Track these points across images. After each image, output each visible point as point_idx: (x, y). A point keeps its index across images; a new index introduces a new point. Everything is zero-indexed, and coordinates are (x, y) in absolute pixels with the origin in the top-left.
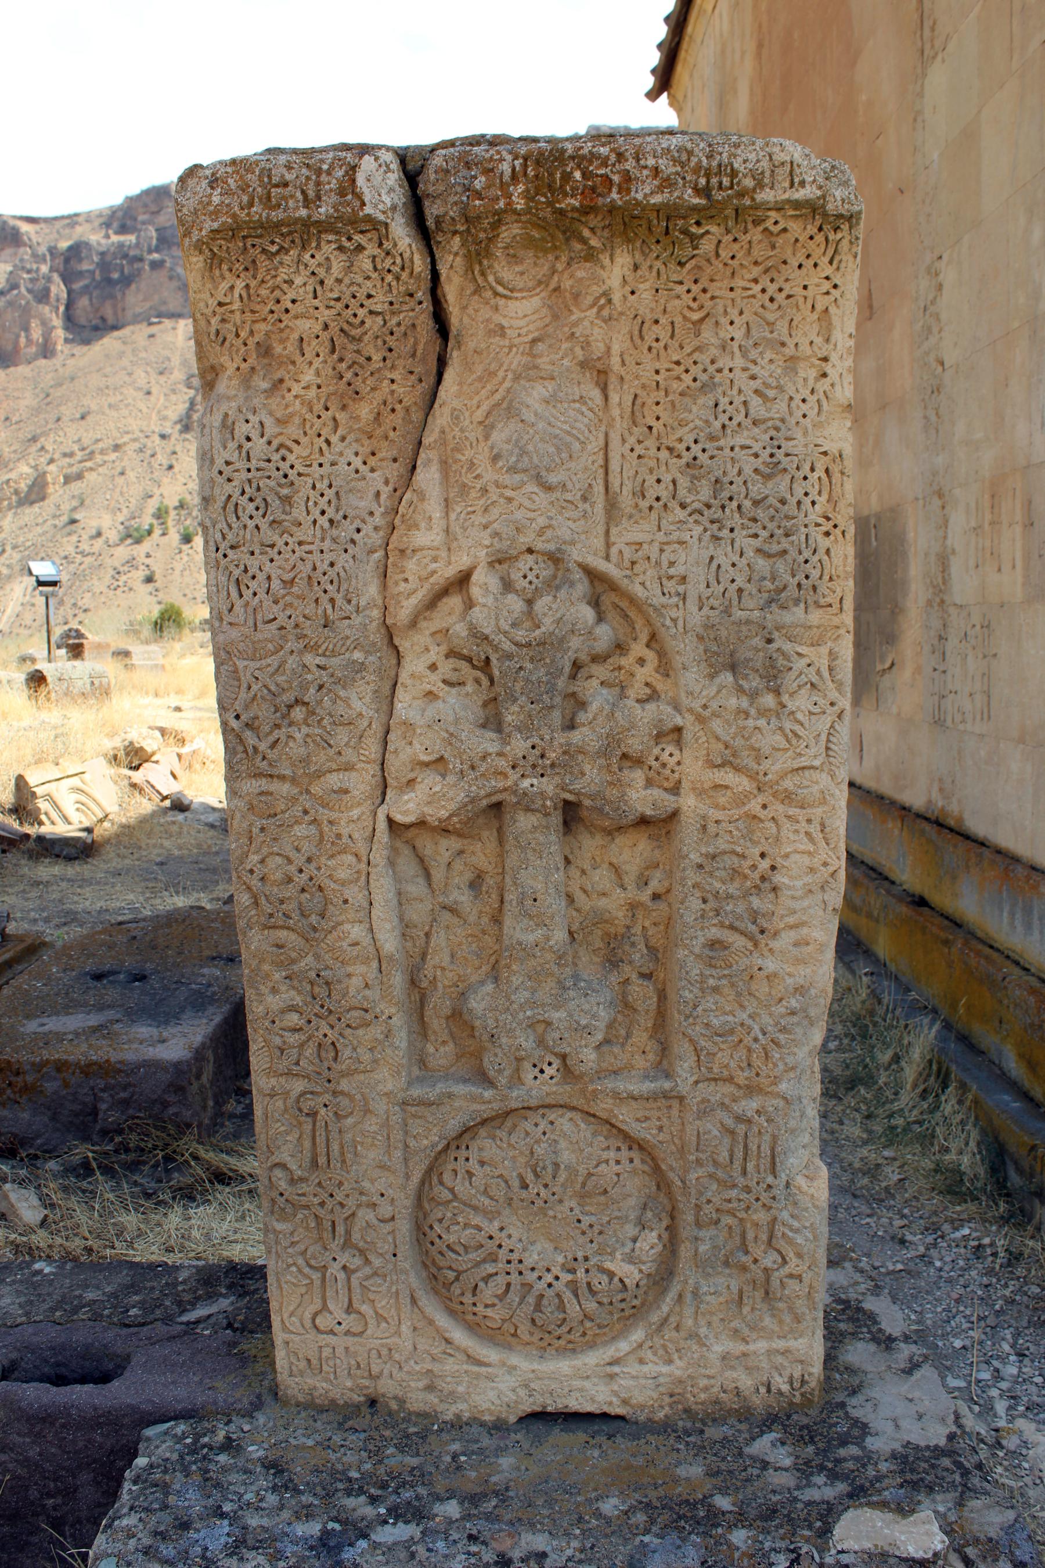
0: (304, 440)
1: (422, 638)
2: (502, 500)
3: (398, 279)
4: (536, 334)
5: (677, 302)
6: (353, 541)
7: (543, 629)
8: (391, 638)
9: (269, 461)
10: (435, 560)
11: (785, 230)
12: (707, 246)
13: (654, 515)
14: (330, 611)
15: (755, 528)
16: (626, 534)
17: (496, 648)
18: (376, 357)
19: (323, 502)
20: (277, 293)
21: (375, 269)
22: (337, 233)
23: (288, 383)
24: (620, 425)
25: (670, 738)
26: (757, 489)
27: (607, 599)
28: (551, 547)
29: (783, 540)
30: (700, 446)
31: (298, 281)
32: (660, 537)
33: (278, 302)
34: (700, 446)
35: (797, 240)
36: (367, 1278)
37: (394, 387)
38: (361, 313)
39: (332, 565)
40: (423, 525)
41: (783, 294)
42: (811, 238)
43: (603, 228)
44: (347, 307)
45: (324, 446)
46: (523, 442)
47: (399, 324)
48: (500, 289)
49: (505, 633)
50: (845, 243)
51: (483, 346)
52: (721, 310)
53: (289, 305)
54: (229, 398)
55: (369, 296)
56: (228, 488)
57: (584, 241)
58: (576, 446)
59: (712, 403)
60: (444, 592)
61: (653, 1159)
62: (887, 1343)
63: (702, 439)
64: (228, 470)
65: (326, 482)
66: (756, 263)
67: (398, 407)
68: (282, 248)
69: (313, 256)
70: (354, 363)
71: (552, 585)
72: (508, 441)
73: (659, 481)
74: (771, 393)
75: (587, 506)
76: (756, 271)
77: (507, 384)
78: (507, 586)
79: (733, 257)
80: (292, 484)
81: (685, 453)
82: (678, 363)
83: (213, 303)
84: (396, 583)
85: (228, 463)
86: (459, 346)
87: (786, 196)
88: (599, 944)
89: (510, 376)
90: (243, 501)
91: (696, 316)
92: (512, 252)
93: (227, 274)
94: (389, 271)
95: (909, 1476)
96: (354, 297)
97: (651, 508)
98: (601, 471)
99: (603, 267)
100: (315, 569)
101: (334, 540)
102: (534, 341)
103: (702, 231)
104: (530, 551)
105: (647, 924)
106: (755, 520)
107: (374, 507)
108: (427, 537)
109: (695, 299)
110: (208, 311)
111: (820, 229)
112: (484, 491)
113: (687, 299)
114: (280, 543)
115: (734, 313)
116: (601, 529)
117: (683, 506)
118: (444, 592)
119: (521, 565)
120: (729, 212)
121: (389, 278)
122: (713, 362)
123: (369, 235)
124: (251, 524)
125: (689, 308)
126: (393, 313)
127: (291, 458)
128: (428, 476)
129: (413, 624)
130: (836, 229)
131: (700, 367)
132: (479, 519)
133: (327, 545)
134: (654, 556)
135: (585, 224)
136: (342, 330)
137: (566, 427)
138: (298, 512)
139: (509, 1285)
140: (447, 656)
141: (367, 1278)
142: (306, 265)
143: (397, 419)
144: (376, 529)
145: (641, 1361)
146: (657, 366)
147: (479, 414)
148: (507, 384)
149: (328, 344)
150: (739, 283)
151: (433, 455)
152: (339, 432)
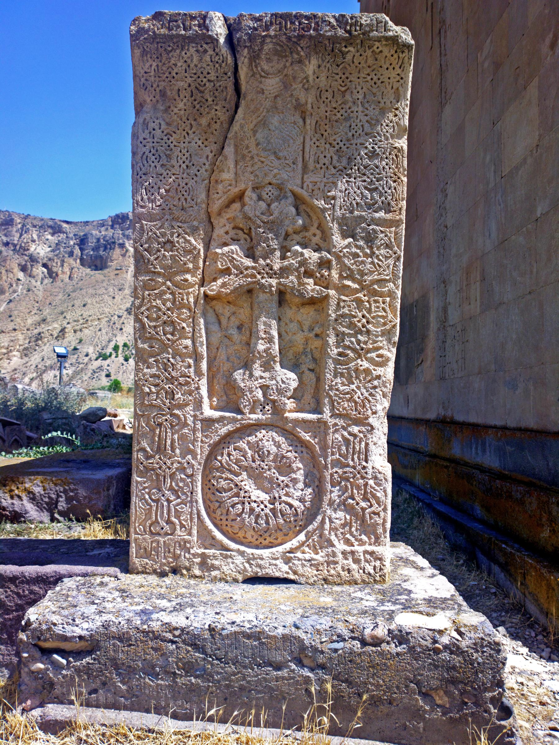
0: (177, 132)
1: (223, 221)
2: (259, 163)
3: (221, 66)
4: (277, 94)
5: (335, 82)
6: (196, 175)
7: (274, 216)
8: (210, 219)
10: (230, 185)
11: (381, 52)
12: (349, 57)
13: (323, 171)
14: (184, 203)
15: (365, 178)
16: (310, 178)
17: (254, 223)
19: (184, 158)
20: (170, 69)
21: (212, 61)
23: (172, 108)
24: (310, 133)
25: (325, 266)
26: (366, 161)
27: (302, 207)
28: (279, 182)
30: (343, 143)
31: (179, 64)
32: (325, 180)
33: (170, 73)
34: (343, 143)
35: (386, 57)
36: (178, 504)
37: (217, 112)
38: (205, 80)
39: (186, 184)
40: (226, 170)
41: (380, 81)
42: (392, 56)
44: (199, 77)
45: (186, 135)
46: (269, 138)
47: (220, 86)
48: (263, 74)
49: (258, 217)
50: (406, 58)
51: (254, 97)
52: (354, 86)
53: (175, 75)
54: (147, 113)
55: (208, 73)
56: (144, 149)
57: (298, 53)
58: (291, 141)
59: (348, 125)
60: (232, 201)
61: (312, 453)
63: (344, 140)
64: (144, 142)
65: (186, 150)
66: (369, 67)
67: (218, 121)
68: (173, 49)
69: (186, 54)
70: (200, 101)
71: (278, 199)
72: (263, 138)
73: (325, 157)
74: (373, 122)
75: (295, 166)
76: (368, 71)
77: (264, 114)
78: (260, 198)
79: (360, 63)
80: (171, 150)
81: (336, 146)
82: (335, 108)
83: (142, 72)
84: (214, 194)
85: (144, 139)
86: (245, 98)
87: (382, 35)
88: (291, 357)
89: (265, 110)
90: (150, 155)
91: (343, 89)
92: (268, 57)
93: (149, 59)
94: (217, 62)
95: (432, 605)
96: (202, 73)
97: (321, 168)
98: (301, 153)
100: (179, 185)
101: (188, 174)
102: (276, 97)
103: (347, 50)
104: (270, 184)
105: (313, 347)
107: (205, 161)
108: (227, 176)
110: (141, 75)
111: (396, 52)
112: (252, 158)
113: (340, 81)
114: (165, 173)
115: (359, 88)
116: (300, 176)
117: (335, 168)
118: (232, 201)
119: (266, 189)
120: (359, 41)
121: (217, 65)
122: (349, 108)
124: (153, 165)
125: (341, 85)
126: (218, 81)
127: (172, 139)
128: (229, 150)
129: (219, 214)
130: (403, 52)
131: (344, 110)
132: (249, 169)
133: (185, 175)
134: (322, 187)
135: (299, 45)
136: (196, 87)
137: (288, 133)
138: (174, 162)
140: (233, 228)
141: (178, 504)
142: (183, 58)
143: (217, 126)
144: (206, 171)
145: (303, 552)
146: (327, 109)
147: (252, 126)
148: (264, 114)
149: (190, 92)
151: (232, 142)
152: (193, 130)
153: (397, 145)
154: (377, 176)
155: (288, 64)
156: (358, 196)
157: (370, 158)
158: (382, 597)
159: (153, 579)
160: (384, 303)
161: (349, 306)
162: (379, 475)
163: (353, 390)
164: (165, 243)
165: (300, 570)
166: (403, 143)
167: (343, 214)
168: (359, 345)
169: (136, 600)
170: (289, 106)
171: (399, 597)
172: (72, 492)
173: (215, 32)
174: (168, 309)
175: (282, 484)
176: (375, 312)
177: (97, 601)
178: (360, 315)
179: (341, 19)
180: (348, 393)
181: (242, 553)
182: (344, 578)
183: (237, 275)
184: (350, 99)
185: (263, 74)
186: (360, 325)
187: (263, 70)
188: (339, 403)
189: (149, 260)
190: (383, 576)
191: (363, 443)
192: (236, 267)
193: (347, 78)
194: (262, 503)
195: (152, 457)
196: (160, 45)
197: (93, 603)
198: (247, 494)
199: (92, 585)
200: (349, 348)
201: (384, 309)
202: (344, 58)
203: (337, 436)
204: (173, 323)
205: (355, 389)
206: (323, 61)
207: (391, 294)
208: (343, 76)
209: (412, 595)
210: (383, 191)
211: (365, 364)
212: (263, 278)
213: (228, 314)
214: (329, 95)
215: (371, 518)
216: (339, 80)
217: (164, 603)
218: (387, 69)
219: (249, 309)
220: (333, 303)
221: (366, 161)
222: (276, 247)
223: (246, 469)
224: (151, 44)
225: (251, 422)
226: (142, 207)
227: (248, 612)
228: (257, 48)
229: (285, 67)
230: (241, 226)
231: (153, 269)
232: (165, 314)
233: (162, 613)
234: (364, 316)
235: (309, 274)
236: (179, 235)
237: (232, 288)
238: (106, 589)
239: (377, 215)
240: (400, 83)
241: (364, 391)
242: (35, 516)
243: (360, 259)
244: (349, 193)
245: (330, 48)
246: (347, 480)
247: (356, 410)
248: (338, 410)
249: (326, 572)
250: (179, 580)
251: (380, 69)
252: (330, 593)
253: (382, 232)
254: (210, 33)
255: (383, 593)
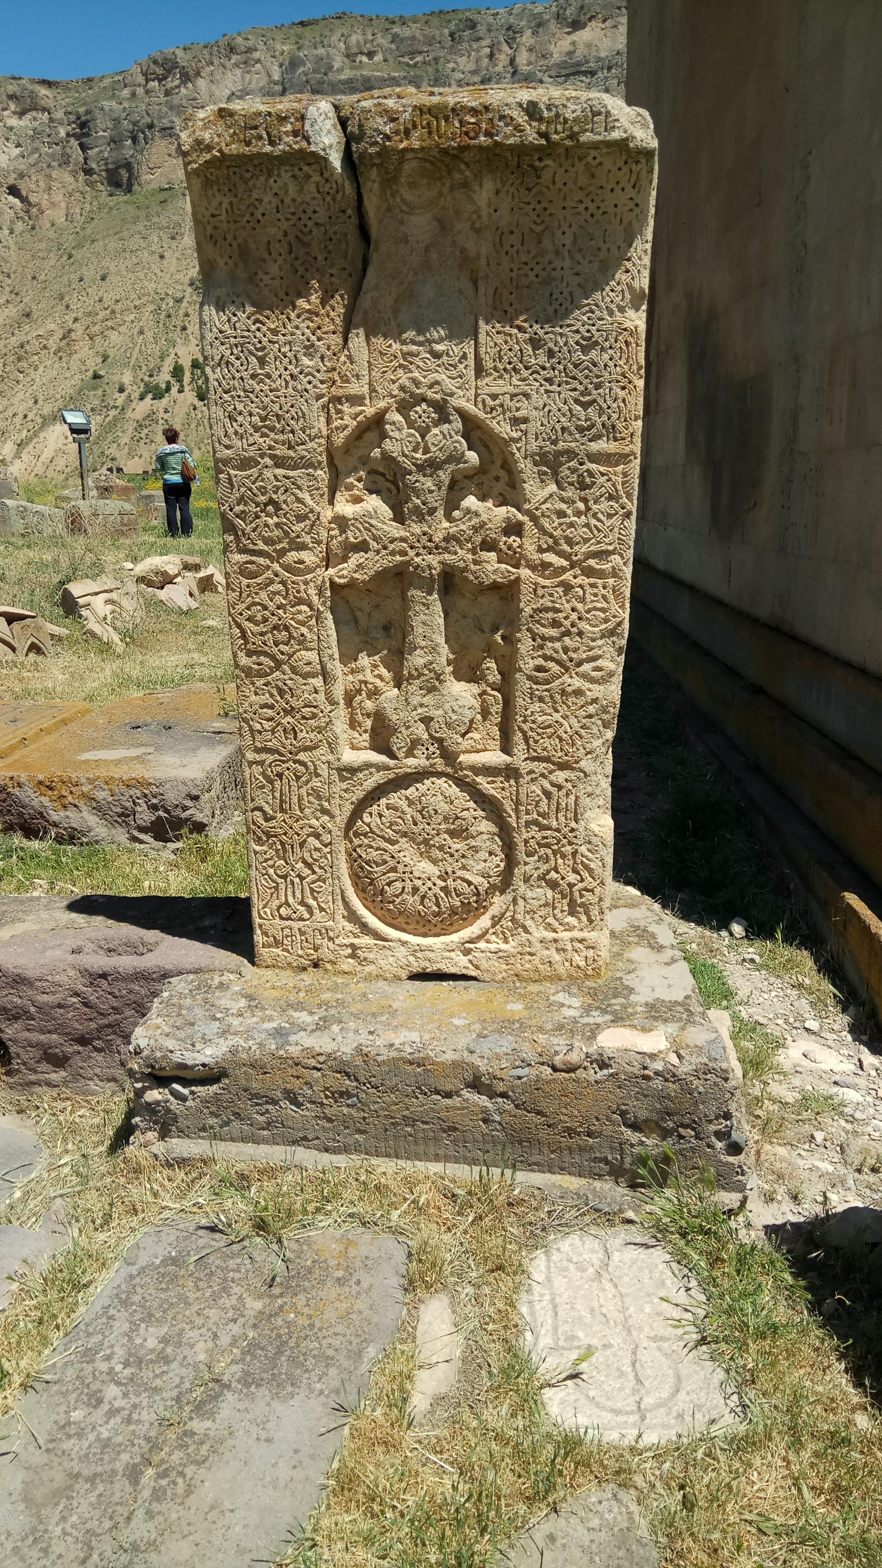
3: (334, 200)
9: (249, 331)
11: (601, 164)
12: (547, 176)
18: (320, 258)
20: (252, 209)
21: (319, 192)
22: (292, 165)
23: (260, 275)
27: (476, 434)
29: (594, 392)
31: (266, 199)
33: (252, 214)
35: (610, 171)
36: (314, 882)
37: (333, 279)
43: (475, 162)
47: (335, 233)
48: (405, 208)
50: (644, 172)
52: (557, 223)
53: (260, 217)
55: (315, 212)
57: (461, 172)
59: (548, 294)
62: (660, 948)
66: (581, 188)
76: (581, 195)
83: (207, 214)
89: (411, 273)
91: (538, 229)
96: (305, 212)
99: (474, 192)
102: (427, 249)
103: (542, 164)
106: (574, 378)
109: (538, 216)
111: (626, 163)
120: (561, 150)
121: (328, 199)
123: (314, 167)
125: (535, 222)
130: (637, 162)
139: (404, 888)
141: (314, 882)
142: (271, 188)
145: (488, 942)
150: (570, 203)
153: (628, 324)
154: (595, 380)
155: (445, 190)
156: (564, 415)
157: (585, 350)
158: (591, 1002)
159: (287, 978)
160: (604, 588)
161: (551, 595)
162: (594, 840)
163: (557, 722)
164: (266, 505)
165: (484, 964)
166: (637, 320)
167: (541, 448)
168: (566, 654)
169: (267, 1012)
170: (449, 262)
171: (613, 1001)
172: (155, 797)
173: (321, 145)
174: (278, 608)
175: (456, 854)
176: (592, 601)
177: (219, 1015)
178: (568, 606)
179: (531, 110)
180: (550, 726)
181: (404, 943)
182: (544, 973)
183: (378, 552)
184: (551, 247)
185: (405, 208)
186: (567, 623)
187: (404, 201)
188: (536, 742)
189: (243, 531)
190: (597, 972)
191: (573, 797)
192: (375, 538)
193: (545, 209)
194: (429, 879)
195: (273, 818)
196: (232, 170)
197: (215, 1019)
198: (408, 869)
199: (210, 987)
200: (552, 659)
201: (604, 597)
202: (539, 177)
203: (534, 788)
204: (286, 628)
205: (561, 720)
206: (504, 183)
207: (615, 573)
208: (538, 207)
209: (633, 998)
210: (604, 406)
211: (577, 683)
212: (418, 555)
213: (368, 609)
214: (515, 239)
215: (581, 896)
216: (531, 213)
217: (303, 1017)
218: (612, 190)
219: (399, 600)
220: (525, 589)
221: (579, 355)
222: (437, 505)
223: (405, 835)
224: (218, 169)
225: (409, 770)
226: (228, 447)
227: (410, 1029)
228: (392, 168)
229: (441, 194)
230: (381, 469)
231: (251, 546)
232: (273, 615)
233: (303, 1033)
234: (573, 610)
235: (488, 545)
236: (286, 491)
237: (372, 573)
238: (228, 995)
239: (595, 447)
240: (634, 213)
241: (573, 721)
242: (103, 835)
243: (567, 520)
244: (550, 411)
245: (515, 163)
246: (548, 846)
247: (562, 750)
248: (535, 751)
249: (519, 966)
250: (323, 978)
251: (599, 191)
252: (522, 997)
253: (603, 474)
254: (313, 148)
255: (593, 993)
